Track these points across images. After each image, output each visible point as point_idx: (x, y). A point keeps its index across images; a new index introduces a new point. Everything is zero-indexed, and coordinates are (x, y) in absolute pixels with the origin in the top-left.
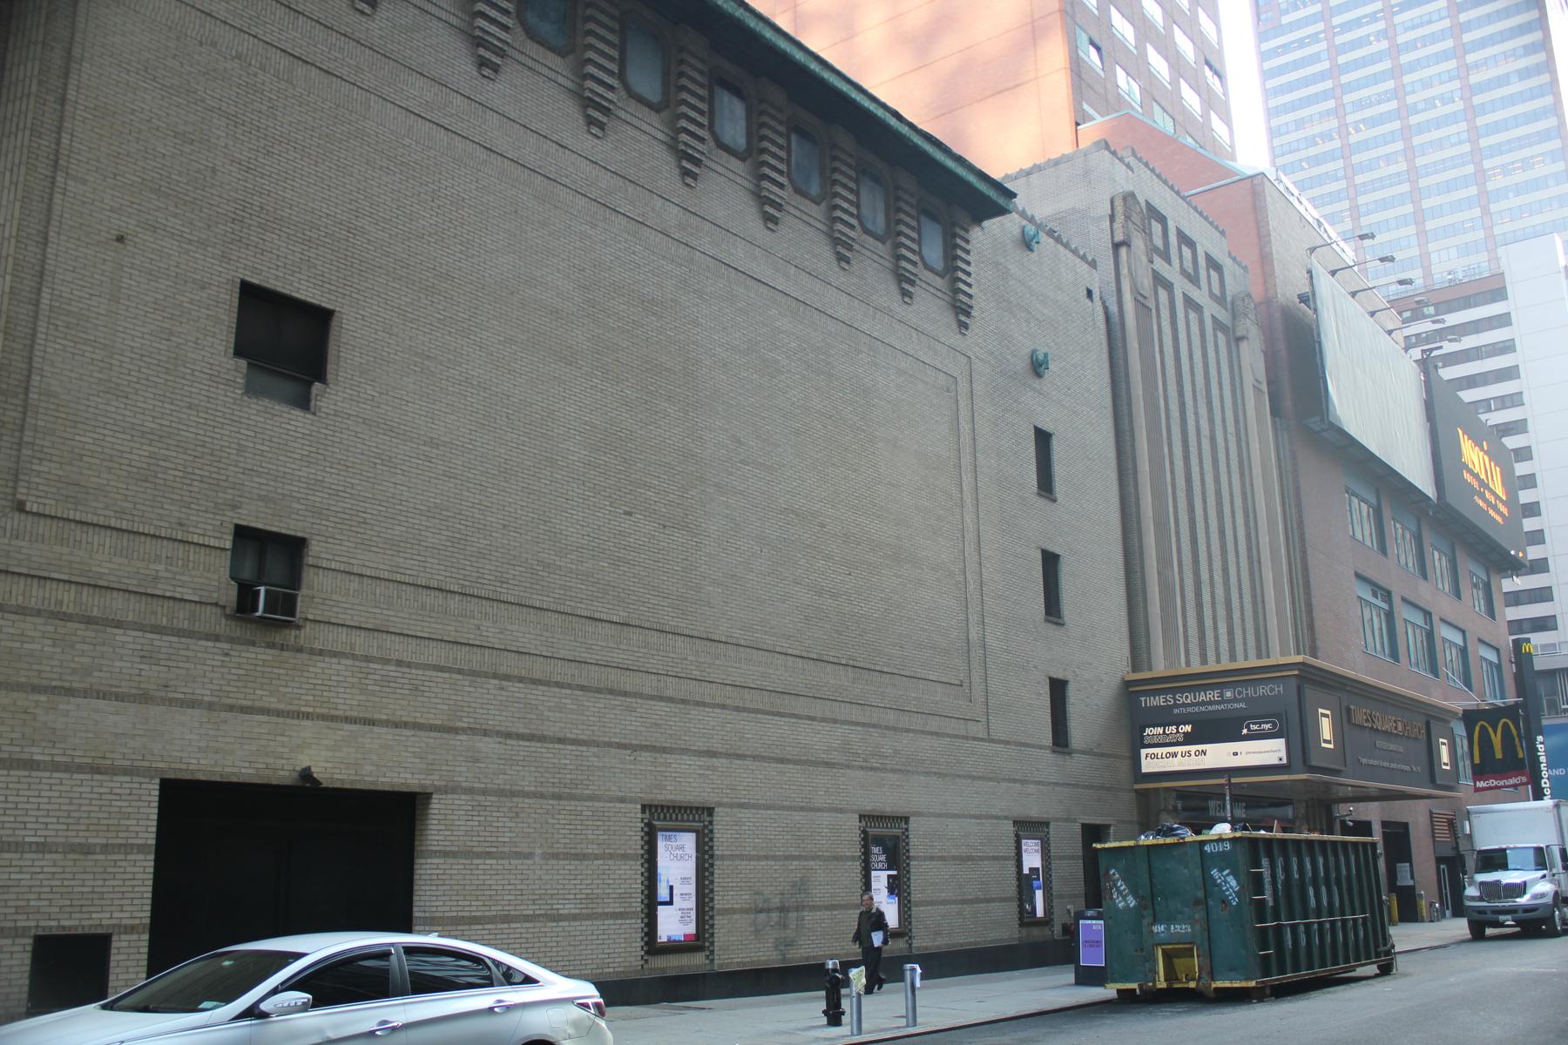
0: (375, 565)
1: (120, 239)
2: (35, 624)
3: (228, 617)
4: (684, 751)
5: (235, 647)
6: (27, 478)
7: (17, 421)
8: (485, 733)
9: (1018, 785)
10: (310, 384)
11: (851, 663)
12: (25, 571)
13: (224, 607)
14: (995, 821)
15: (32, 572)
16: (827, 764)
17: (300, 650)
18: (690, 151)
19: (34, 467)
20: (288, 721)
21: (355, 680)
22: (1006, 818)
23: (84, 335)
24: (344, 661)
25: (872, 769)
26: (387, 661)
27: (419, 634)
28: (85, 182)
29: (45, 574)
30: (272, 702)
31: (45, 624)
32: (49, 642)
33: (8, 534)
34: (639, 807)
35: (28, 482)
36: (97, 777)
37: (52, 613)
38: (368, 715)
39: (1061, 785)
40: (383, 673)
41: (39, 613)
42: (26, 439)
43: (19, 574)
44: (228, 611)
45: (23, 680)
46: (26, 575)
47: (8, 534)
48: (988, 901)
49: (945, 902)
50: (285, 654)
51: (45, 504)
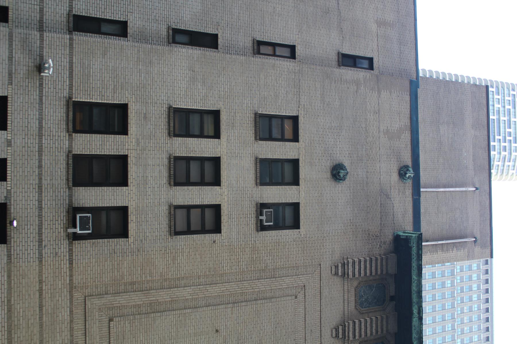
1: (217, 331)
2: (67, 335)
6: (122, 320)
7: (142, 312)
12: (87, 327)
15: (87, 330)
19: (127, 322)
23: (179, 327)
28: (232, 314)
29: (87, 335)
31: (68, 339)
33: (100, 318)
35: (121, 320)
37: (73, 341)
41: (72, 336)
42: (136, 316)
43: (85, 325)
45: (44, 336)
46: (85, 328)
47: (100, 318)
51: (114, 328)
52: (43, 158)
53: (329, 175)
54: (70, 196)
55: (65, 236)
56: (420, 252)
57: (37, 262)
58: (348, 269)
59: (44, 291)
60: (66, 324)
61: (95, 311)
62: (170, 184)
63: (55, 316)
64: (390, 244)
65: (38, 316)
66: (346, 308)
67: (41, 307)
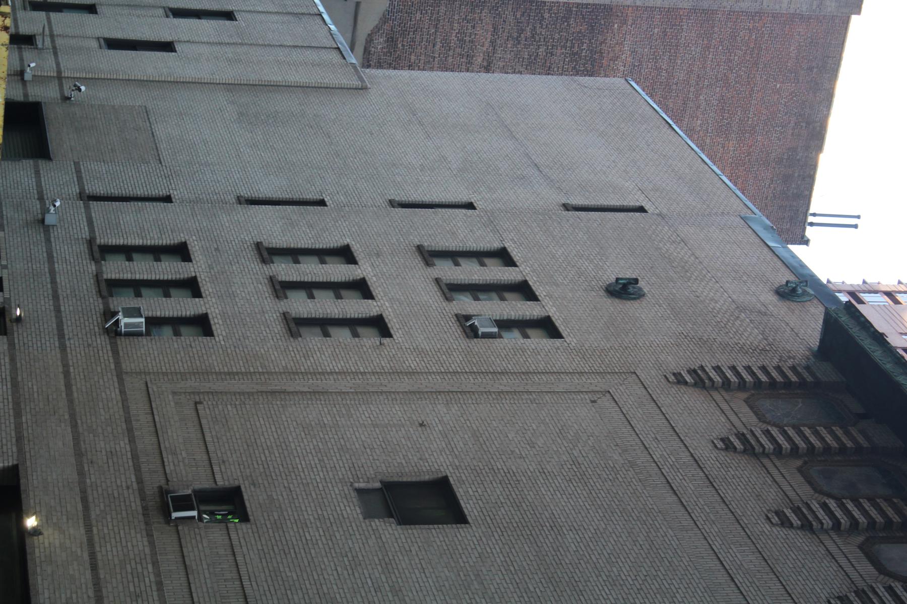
0: (248, 561)
1: (421, 425)
3: (160, 488)
5: (137, 493)
10: (392, 517)
13: (168, 484)
17: (147, 524)
19: (229, 406)
20: (81, 522)
21: (132, 556)
24: (147, 550)
26: (158, 574)
27: (194, 595)
29: (155, 412)
30: (94, 514)
32: (108, 417)
36: (14, 440)
38: (100, 564)
40: (145, 573)
44: (165, 487)
50: (141, 517)
52: (58, 276)
53: (602, 293)
54: (106, 305)
55: (102, 333)
56: (862, 319)
57: (58, 350)
58: (707, 373)
59: (72, 374)
60: (115, 402)
61: (165, 393)
62: (278, 297)
63: (94, 394)
64: (808, 359)
65: (64, 395)
66: (733, 418)
67: (68, 386)
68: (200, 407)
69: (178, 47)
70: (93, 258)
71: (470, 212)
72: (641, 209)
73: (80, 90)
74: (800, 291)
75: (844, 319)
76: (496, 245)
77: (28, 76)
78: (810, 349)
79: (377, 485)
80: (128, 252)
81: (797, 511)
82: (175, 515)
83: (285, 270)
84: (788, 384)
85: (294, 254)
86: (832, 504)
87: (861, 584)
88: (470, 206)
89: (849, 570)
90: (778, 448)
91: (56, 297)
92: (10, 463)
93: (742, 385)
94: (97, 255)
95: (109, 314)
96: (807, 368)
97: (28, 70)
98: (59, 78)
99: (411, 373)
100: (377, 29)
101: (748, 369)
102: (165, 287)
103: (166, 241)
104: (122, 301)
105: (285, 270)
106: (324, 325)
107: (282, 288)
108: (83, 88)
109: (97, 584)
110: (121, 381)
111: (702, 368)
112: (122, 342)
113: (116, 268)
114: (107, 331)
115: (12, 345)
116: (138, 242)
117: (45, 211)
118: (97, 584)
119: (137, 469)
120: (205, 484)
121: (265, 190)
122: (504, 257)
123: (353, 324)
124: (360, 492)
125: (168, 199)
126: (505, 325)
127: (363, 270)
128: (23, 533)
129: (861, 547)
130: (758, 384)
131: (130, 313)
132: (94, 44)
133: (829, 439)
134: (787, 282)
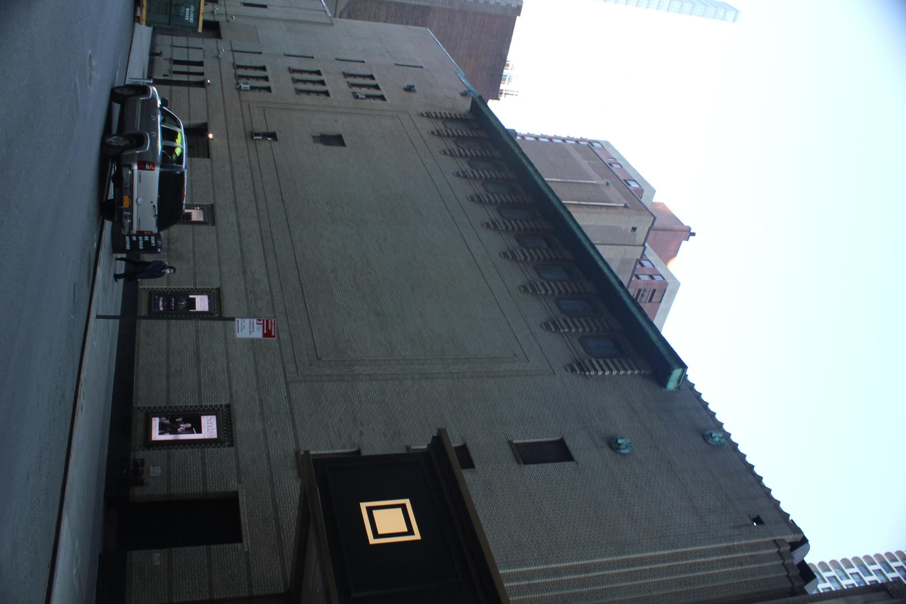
4: (238, 217)
8: (232, 168)
9: (258, 409)
10: (322, 142)
11: (303, 286)
14: (227, 384)
16: (244, 272)
18: (496, 223)
22: (231, 396)
24: (246, 146)
25: (247, 296)
30: (230, 136)
34: (212, 203)
39: (269, 462)
48: (168, 377)
49: (168, 340)
53: (403, 90)
68: (265, 111)
69: (268, 7)
70: (236, 78)
71: (363, 63)
72: (422, 67)
73: (233, 18)
74: (468, 94)
75: (477, 100)
76: (368, 73)
77: (215, 13)
78: (467, 111)
79: (319, 135)
80: (246, 67)
81: (450, 151)
82: (255, 138)
83: (297, 76)
84: (457, 118)
85: (301, 72)
86: (461, 150)
87: (464, 170)
88: (363, 62)
89: (462, 166)
90: (448, 135)
91: (221, 78)
92: (205, 121)
93: (442, 118)
94: (235, 67)
95: (238, 84)
96: (464, 115)
97: (215, 11)
98: (226, 14)
99: (335, 107)
100: (344, 10)
101: (445, 114)
102: (257, 78)
103: (259, 65)
104: (241, 81)
105: (297, 76)
106: (308, 92)
107: (296, 81)
108: (234, 17)
109: (230, 153)
110: (241, 103)
111: (430, 112)
112: (241, 92)
113: (241, 72)
114: (237, 89)
115: (206, 91)
116: (249, 64)
117: (219, 53)
118: (230, 153)
119: (244, 125)
120: (264, 130)
121: (294, 52)
122: (372, 77)
123: (318, 93)
124: (313, 137)
125: (261, 53)
126: (368, 97)
127: (323, 77)
128: (208, 139)
129: (467, 162)
130: (447, 118)
131: (245, 84)
132: (239, 4)
133: (465, 133)
134: (464, 91)
